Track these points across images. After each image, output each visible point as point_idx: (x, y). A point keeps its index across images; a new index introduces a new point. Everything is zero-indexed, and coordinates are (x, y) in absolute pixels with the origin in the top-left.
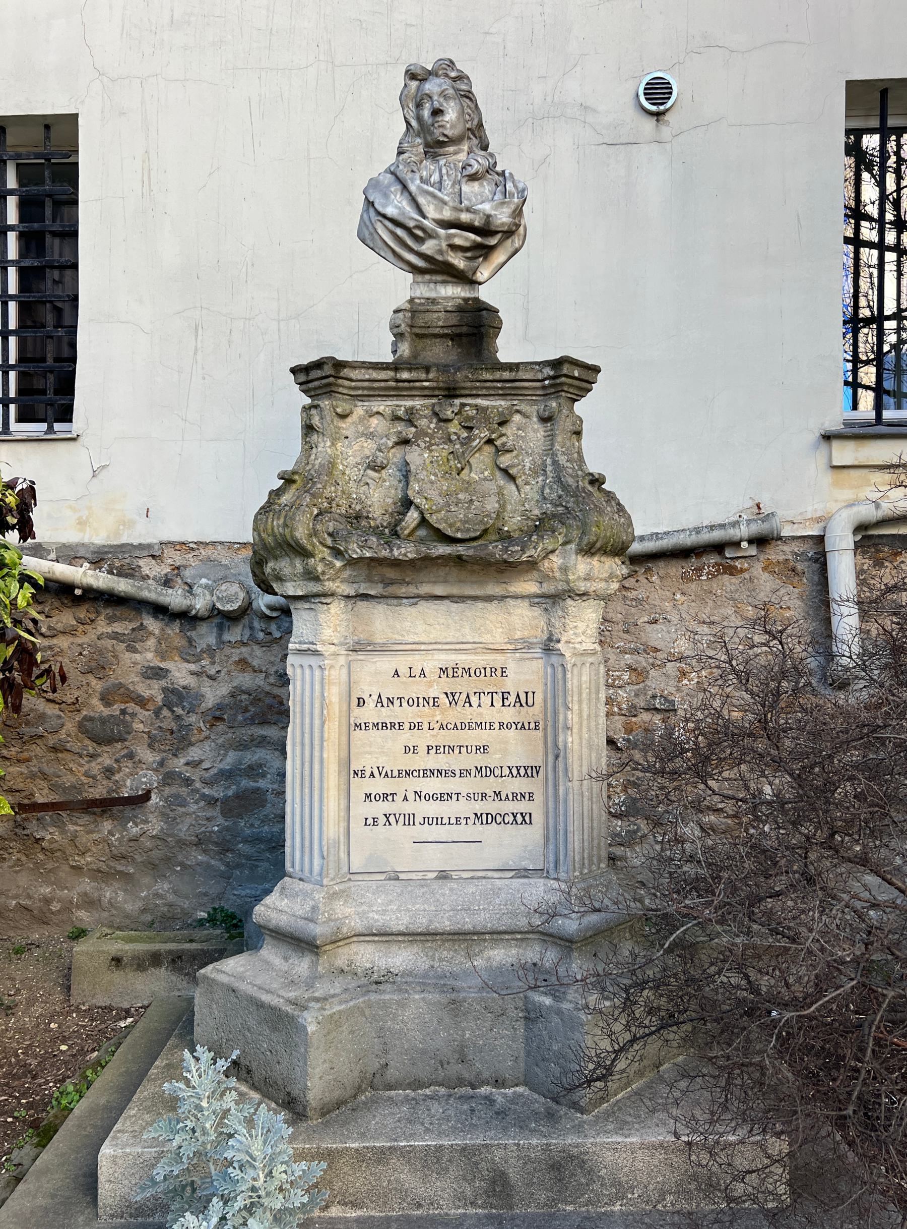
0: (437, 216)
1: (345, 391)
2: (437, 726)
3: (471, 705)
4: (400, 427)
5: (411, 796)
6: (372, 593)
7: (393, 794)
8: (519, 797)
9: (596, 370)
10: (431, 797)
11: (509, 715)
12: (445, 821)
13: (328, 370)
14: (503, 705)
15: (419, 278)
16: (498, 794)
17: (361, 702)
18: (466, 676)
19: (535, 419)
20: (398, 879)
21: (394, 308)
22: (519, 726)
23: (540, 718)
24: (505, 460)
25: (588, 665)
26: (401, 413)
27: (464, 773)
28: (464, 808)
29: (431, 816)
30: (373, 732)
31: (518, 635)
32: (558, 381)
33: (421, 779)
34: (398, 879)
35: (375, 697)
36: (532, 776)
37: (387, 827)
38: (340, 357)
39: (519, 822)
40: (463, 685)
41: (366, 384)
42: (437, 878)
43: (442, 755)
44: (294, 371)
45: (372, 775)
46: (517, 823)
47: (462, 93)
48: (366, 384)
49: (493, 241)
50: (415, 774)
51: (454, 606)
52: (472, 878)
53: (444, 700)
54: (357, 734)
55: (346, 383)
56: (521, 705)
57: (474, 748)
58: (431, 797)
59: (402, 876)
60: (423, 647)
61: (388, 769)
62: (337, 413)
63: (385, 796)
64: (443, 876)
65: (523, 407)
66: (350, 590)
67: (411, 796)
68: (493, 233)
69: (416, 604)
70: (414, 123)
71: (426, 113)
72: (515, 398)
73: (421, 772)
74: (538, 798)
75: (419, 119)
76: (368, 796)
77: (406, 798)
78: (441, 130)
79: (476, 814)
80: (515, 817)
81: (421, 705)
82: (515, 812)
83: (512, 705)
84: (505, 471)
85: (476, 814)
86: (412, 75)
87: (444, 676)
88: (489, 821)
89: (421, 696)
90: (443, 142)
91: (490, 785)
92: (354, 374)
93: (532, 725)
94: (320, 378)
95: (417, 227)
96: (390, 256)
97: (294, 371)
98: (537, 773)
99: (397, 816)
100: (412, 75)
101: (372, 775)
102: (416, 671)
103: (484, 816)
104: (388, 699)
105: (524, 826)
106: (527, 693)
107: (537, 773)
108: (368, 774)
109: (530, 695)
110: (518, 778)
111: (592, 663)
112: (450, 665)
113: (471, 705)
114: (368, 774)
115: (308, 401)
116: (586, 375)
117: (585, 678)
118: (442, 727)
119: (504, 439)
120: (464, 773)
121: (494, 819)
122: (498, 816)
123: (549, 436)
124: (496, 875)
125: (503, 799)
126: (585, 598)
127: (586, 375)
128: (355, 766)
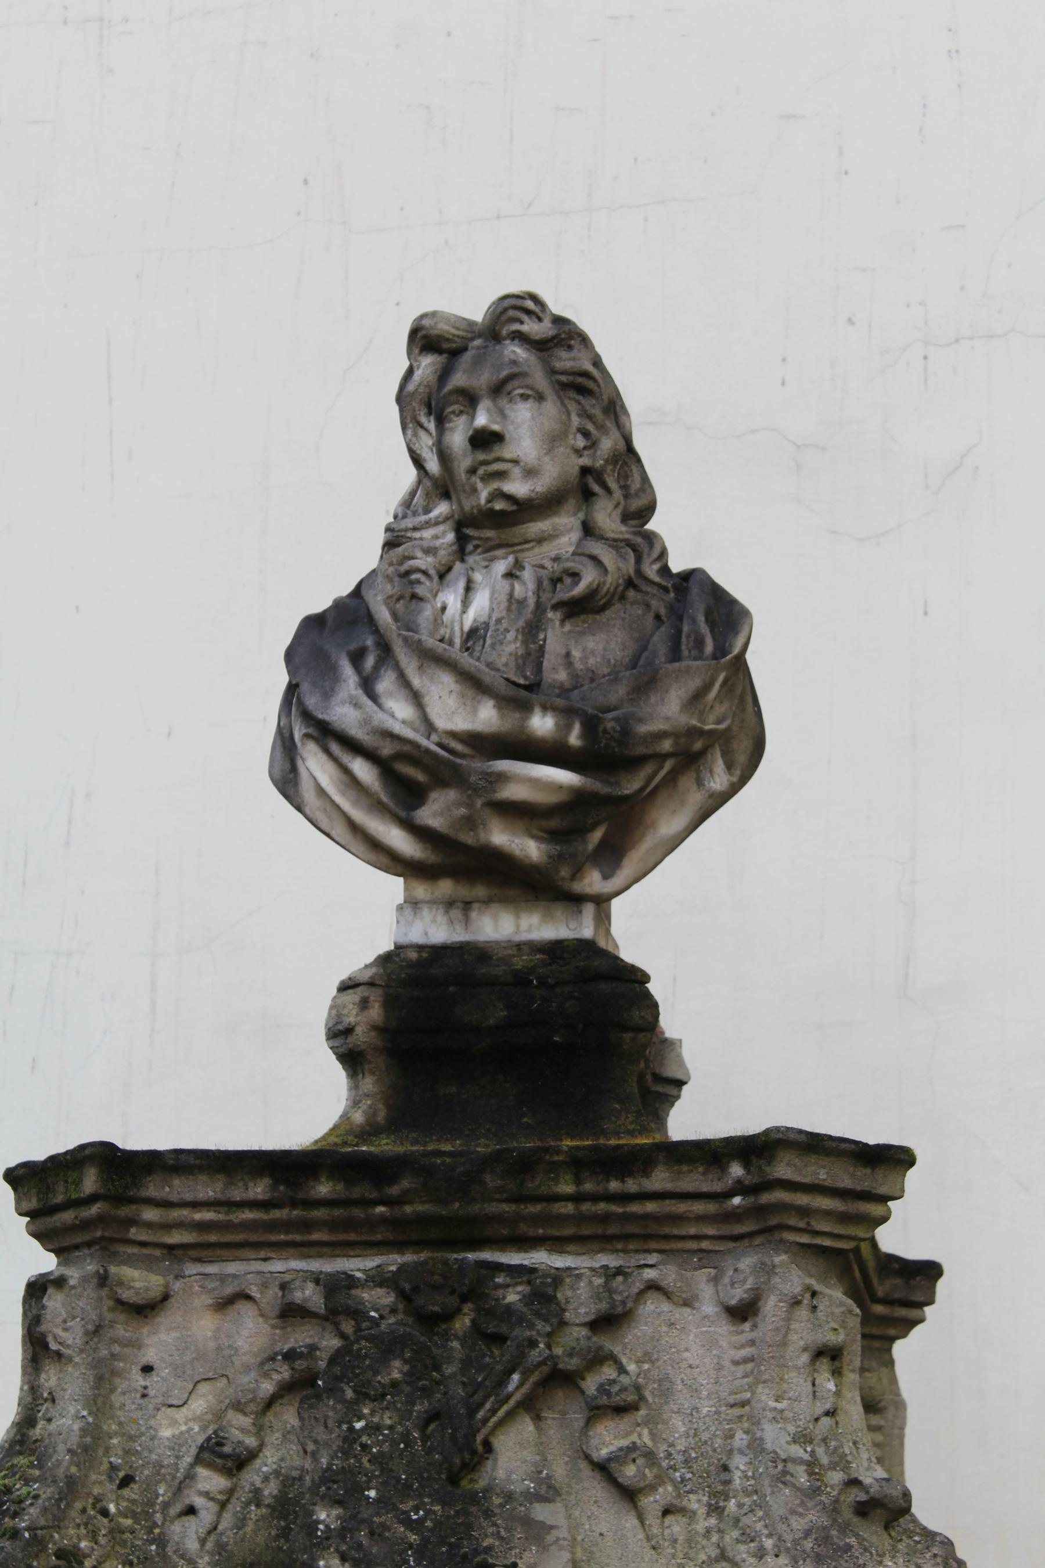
0: (462, 723)
1: (143, 1237)
4: (301, 1337)
9: (895, 1159)
13: (90, 1182)
15: (421, 891)
19: (709, 1308)
21: (344, 975)
24: (608, 1439)
26: (309, 1295)
32: (766, 1198)
38: (134, 1139)
41: (208, 1215)
44: (13, 1177)
47: (563, 378)
48: (208, 1215)
49: (631, 785)
55: (150, 1214)
62: (120, 1302)
65: (668, 1274)
68: (633, 763)
70: (433, 465)
71: (458, 438)
72: (653, 1245)
75: (444, 456)
78: (495, 485)
84: (603, 1469)
86: (424, 339)
90: (502, 513)
92: (179, 1188)
94: (89, 1196)
95: (399, 756)
96: (340, 830)
97: (13, 1177)
100: (424, 339)
115: (46, 1262)
116: (846, 1177)
119: (608, 1372)
123: (746, 1360)
127: (846, 1177)
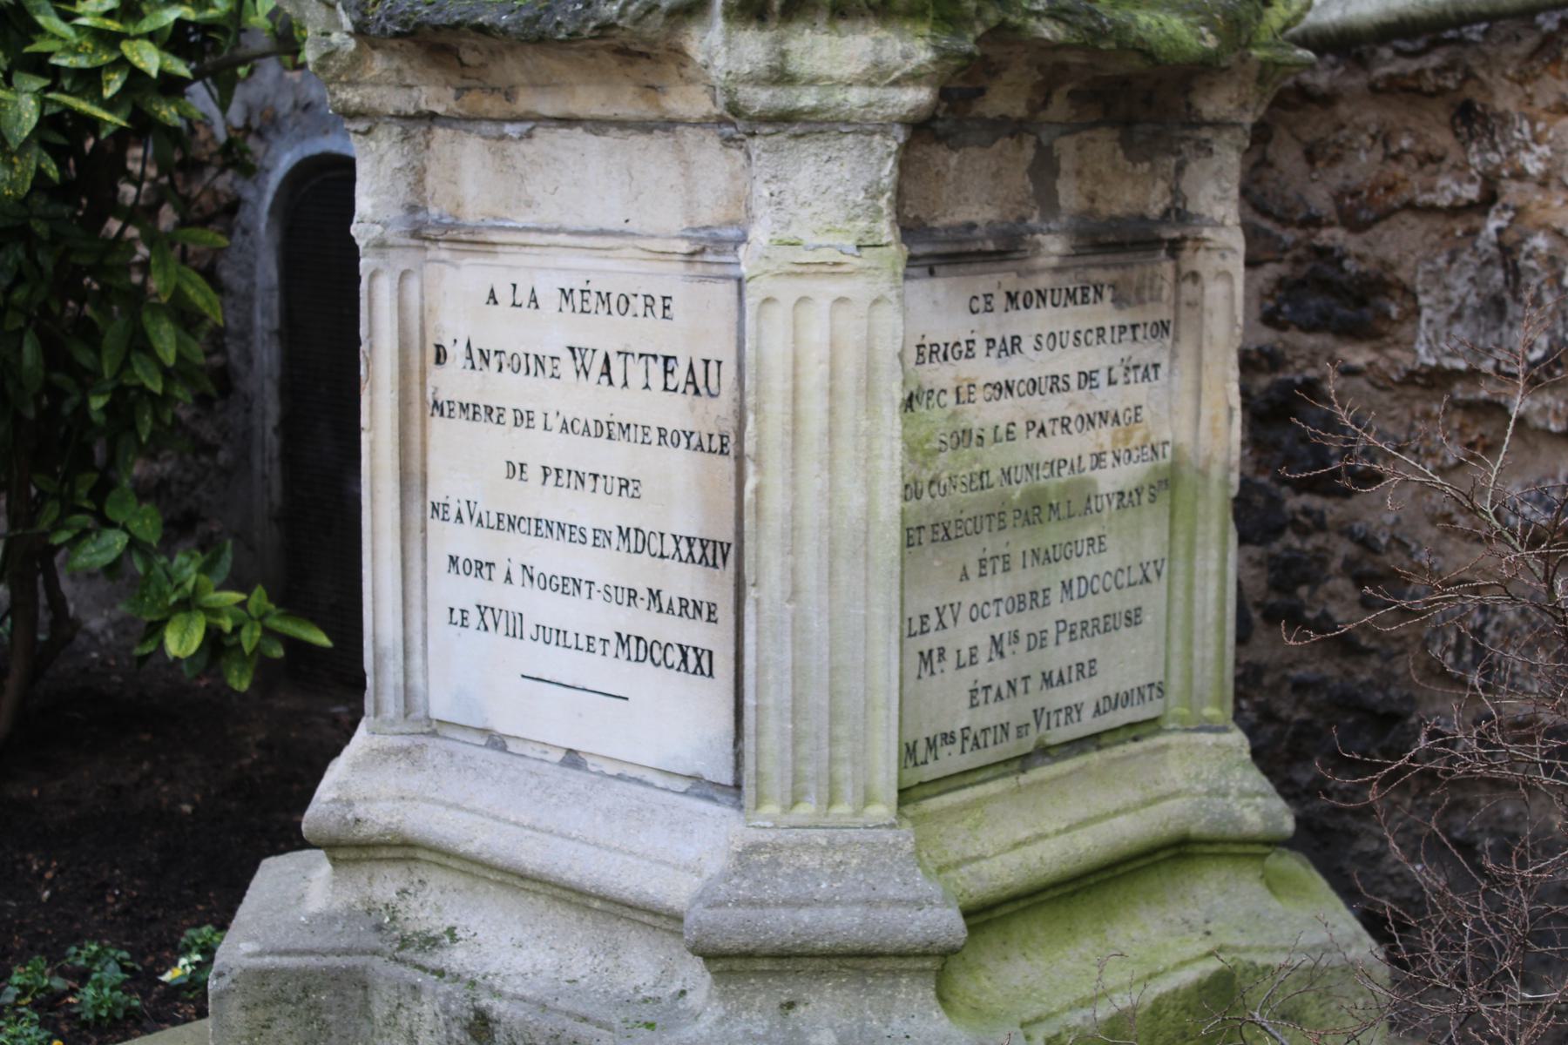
2: (555, 423)
3: (611, 383)
5: (517, 575)
6: (440, 109)
7: (490, 565)
8: (690, 609)
10: (548, 583)
11: (676, 411)
12: (571, 640)
14: (666, 389)
16: (655, 595)
17: (440, 356)
18: (603, 311)
20: (504, 749)
22: (694, 441)
23: (729, 426)
25: (824, 304)
27: (600, 538)
28: (608, 619)
29: (548, 625)
30: (460, 423)
31: (705, 217)
33: (532, 538)
34: (504, 749)
35: (462, 345)
36: (715, 565)
37: (482, 633)
39: (691, 669)
40: (604, 333)
42: (563, 763)
43: (564, 491)
45: (459, 517)
46: (686, 670)
50: (524, 525)
51: (593, 144)
52: (619, 777)
53: (567, 366)
54: (437, 424)
56: (697, 392)
57: (617, 483)
58: (548, 583)
59: (512, 746)
60: (533, 238)
61: (480, 509)
63: (480, 565)
64: (573, 759)
66: (396, 100)
67: (517, 575)
69: (528, 135)
73: (533, 523)
74: (726, 614)
76: (453, 560)
77: (508, 578)
79: (619, 635)
80: (685, 655)
81: (532, 371)
82: (684, 643)
83: (681, 389)
85: (619, 635)
87: (567, 308)
88: (641, 657)
89: (531, 352)
91: (641, 572)
93: (716, 444)
98: (725, 557)
99: (497, 612)
101: (459, 517)
102: (523, 296)
103: (633, 641)
104: (481, 351)
105: (698, 678)
106: (707, 362)
107: (725, 557)
108: (453, 514)
109: (713, 367)
110: (690, 566)
111: (841, 300)
112: (578, 285)
113: (611, 383)
114: (453, 514)
117: (816, 334)
118: (564, 428)
120: (600, 538)
121: (649, 650)
122: (656, 646)
124: (660, 781)
125: (665, 608)
126: (797, 129)
128: (435, 495)
